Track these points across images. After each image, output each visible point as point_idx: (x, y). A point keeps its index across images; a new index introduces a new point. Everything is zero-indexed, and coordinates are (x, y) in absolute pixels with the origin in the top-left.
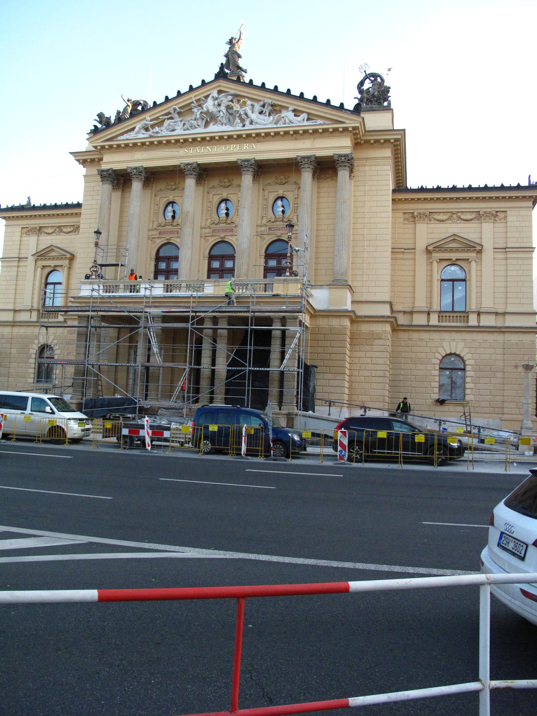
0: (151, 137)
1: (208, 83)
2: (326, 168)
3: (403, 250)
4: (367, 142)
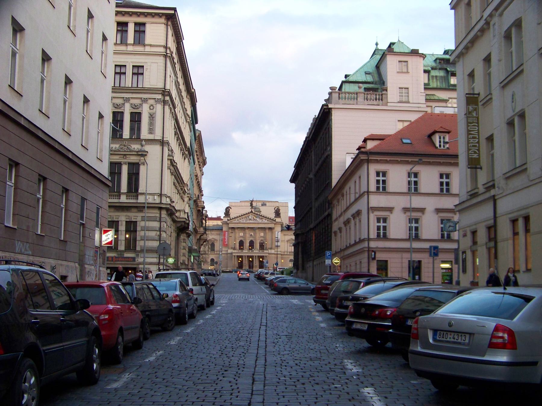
2: (270, 229)
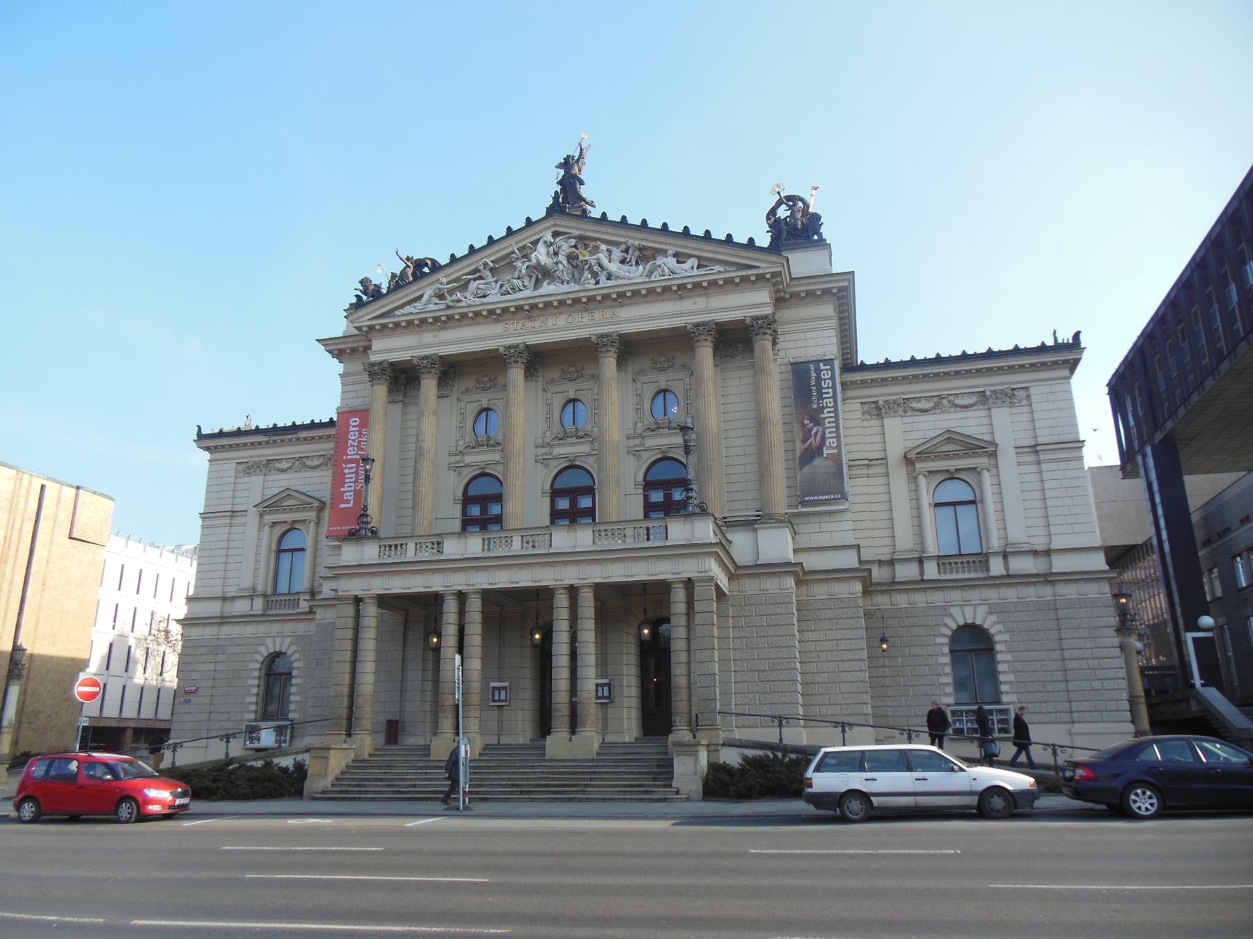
0: (448, 307)
1: (537, 222)
2: (735, 340)
3: (866, 462)
4: (795, 295)
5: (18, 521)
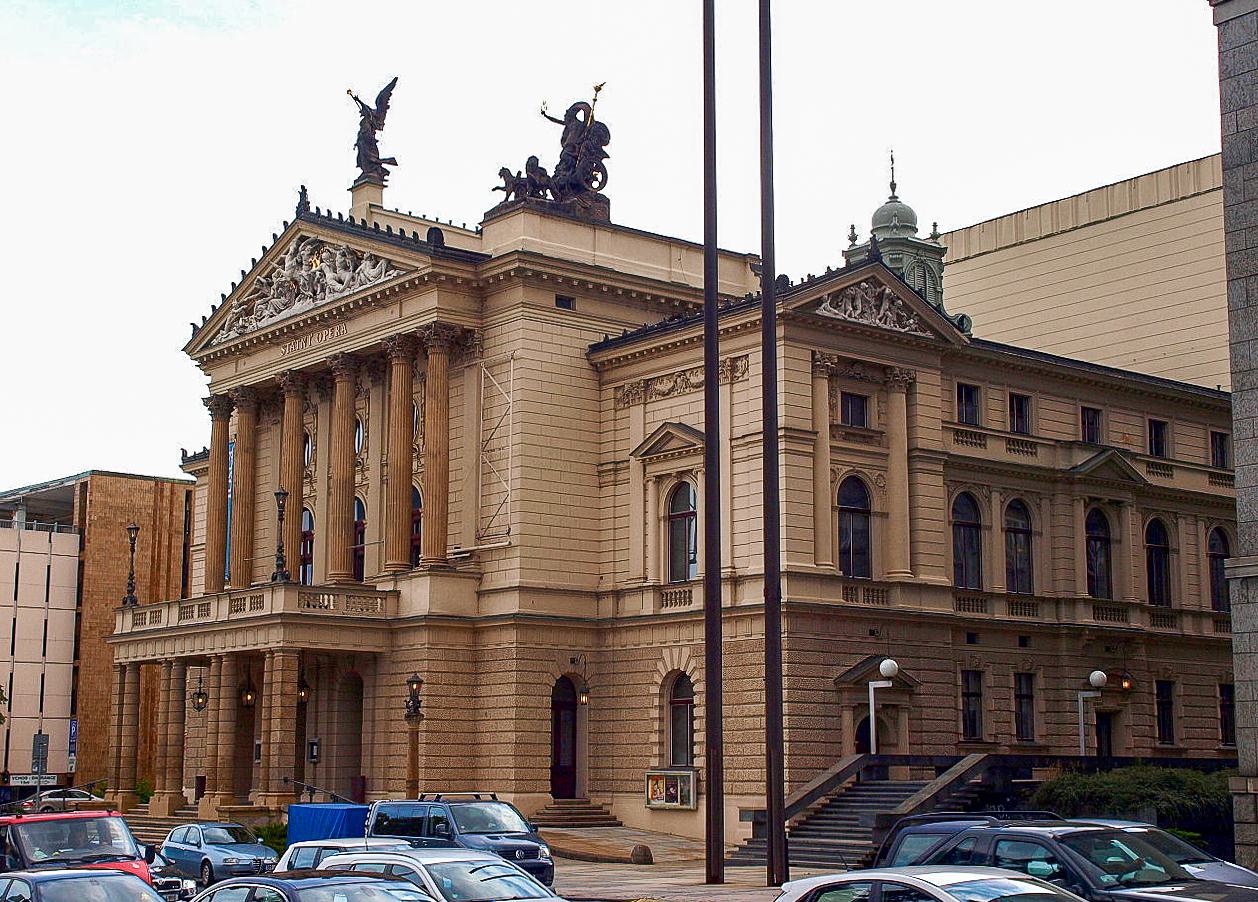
3: (611, 466)
5: (165, 536)
